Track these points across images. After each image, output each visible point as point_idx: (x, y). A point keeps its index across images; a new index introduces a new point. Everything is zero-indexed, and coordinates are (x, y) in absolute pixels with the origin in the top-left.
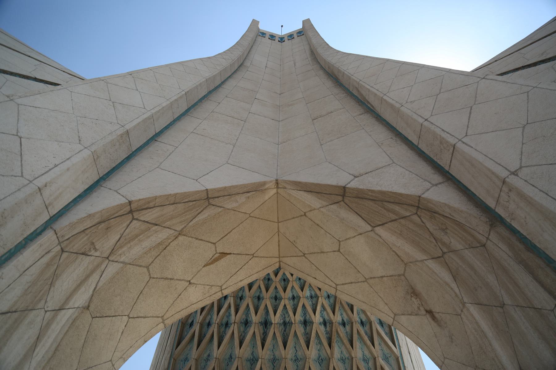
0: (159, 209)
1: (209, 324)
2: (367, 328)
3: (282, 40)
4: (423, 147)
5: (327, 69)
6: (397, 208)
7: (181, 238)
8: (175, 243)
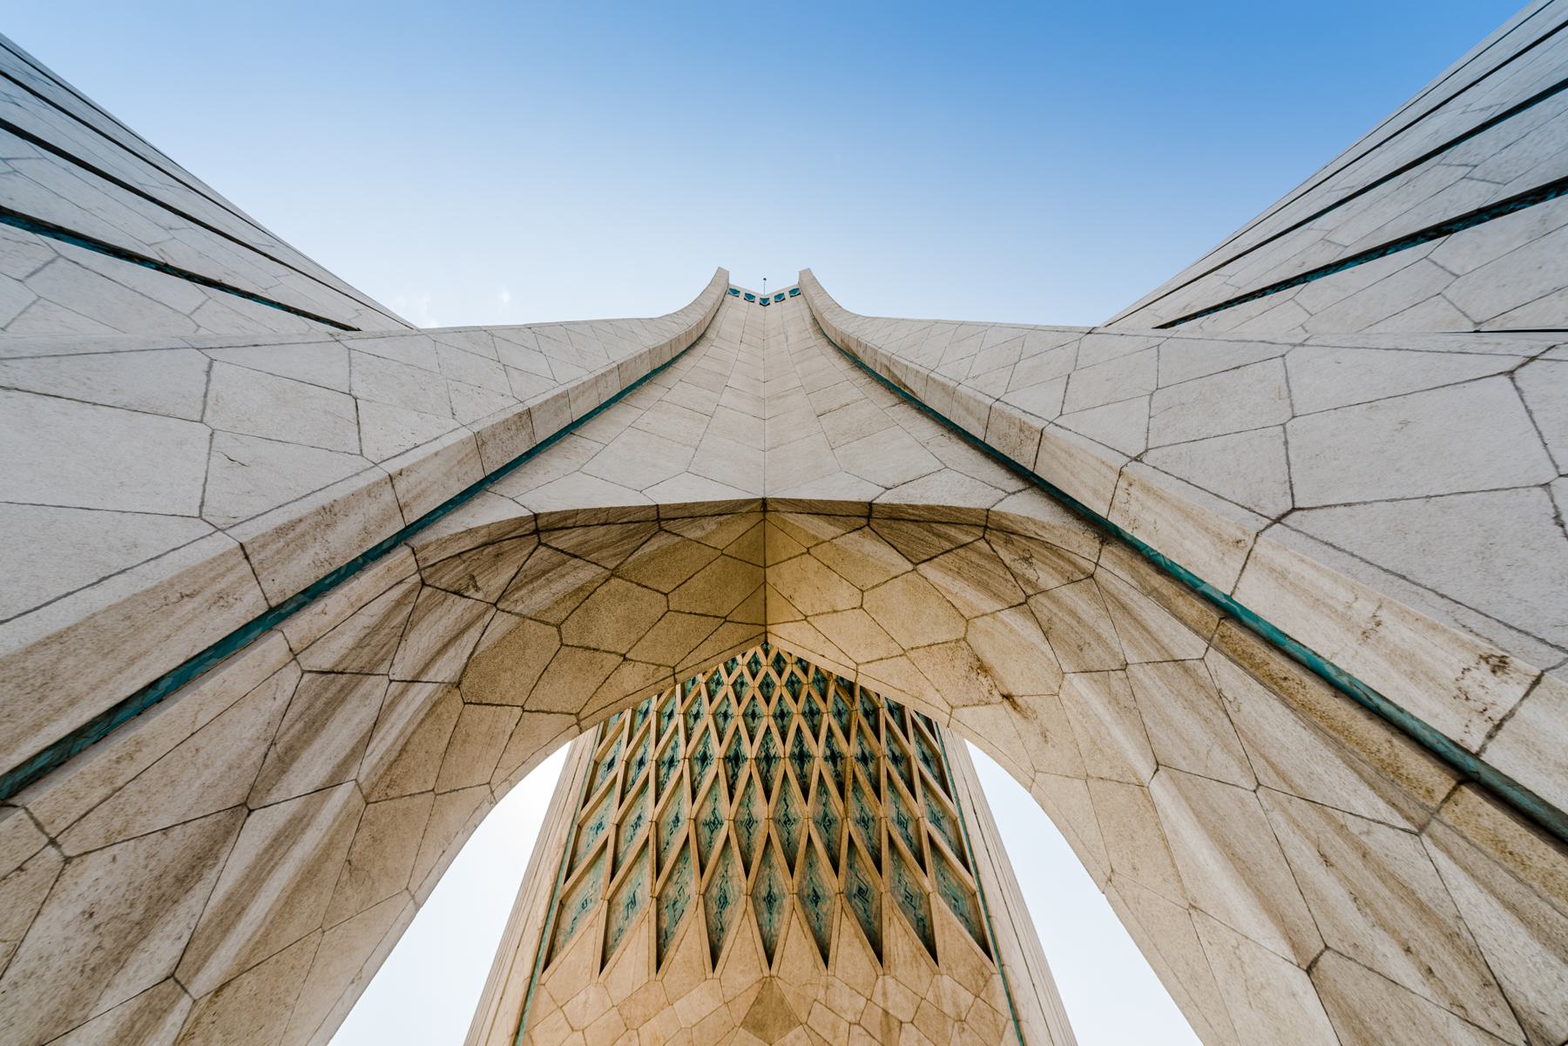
0: (580, 531)
1: (641, 763)
2: (903, 767)
3: (765, 302)
4: (992, 441)
5: (839, 343)
6: (952, 532)
7: (614, 581)
8: (605, 588)
